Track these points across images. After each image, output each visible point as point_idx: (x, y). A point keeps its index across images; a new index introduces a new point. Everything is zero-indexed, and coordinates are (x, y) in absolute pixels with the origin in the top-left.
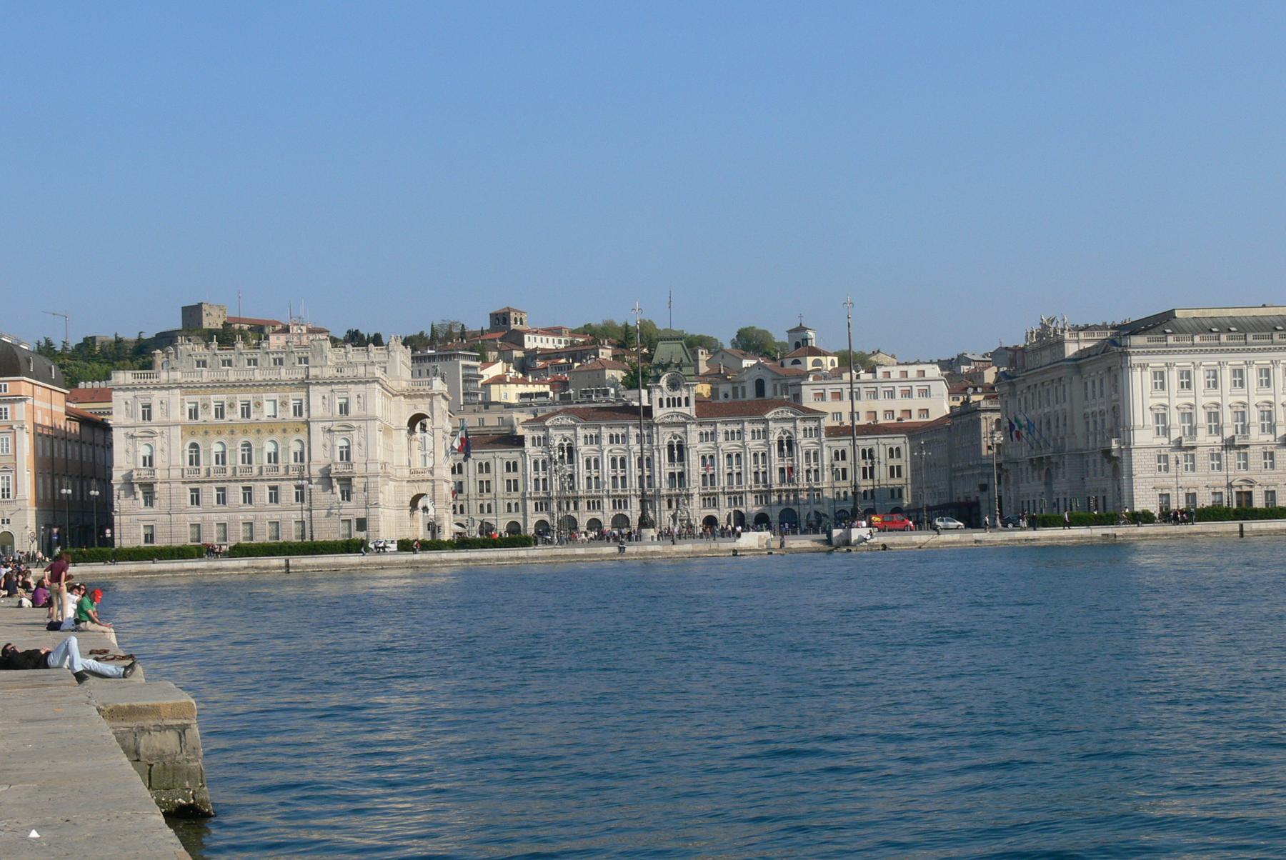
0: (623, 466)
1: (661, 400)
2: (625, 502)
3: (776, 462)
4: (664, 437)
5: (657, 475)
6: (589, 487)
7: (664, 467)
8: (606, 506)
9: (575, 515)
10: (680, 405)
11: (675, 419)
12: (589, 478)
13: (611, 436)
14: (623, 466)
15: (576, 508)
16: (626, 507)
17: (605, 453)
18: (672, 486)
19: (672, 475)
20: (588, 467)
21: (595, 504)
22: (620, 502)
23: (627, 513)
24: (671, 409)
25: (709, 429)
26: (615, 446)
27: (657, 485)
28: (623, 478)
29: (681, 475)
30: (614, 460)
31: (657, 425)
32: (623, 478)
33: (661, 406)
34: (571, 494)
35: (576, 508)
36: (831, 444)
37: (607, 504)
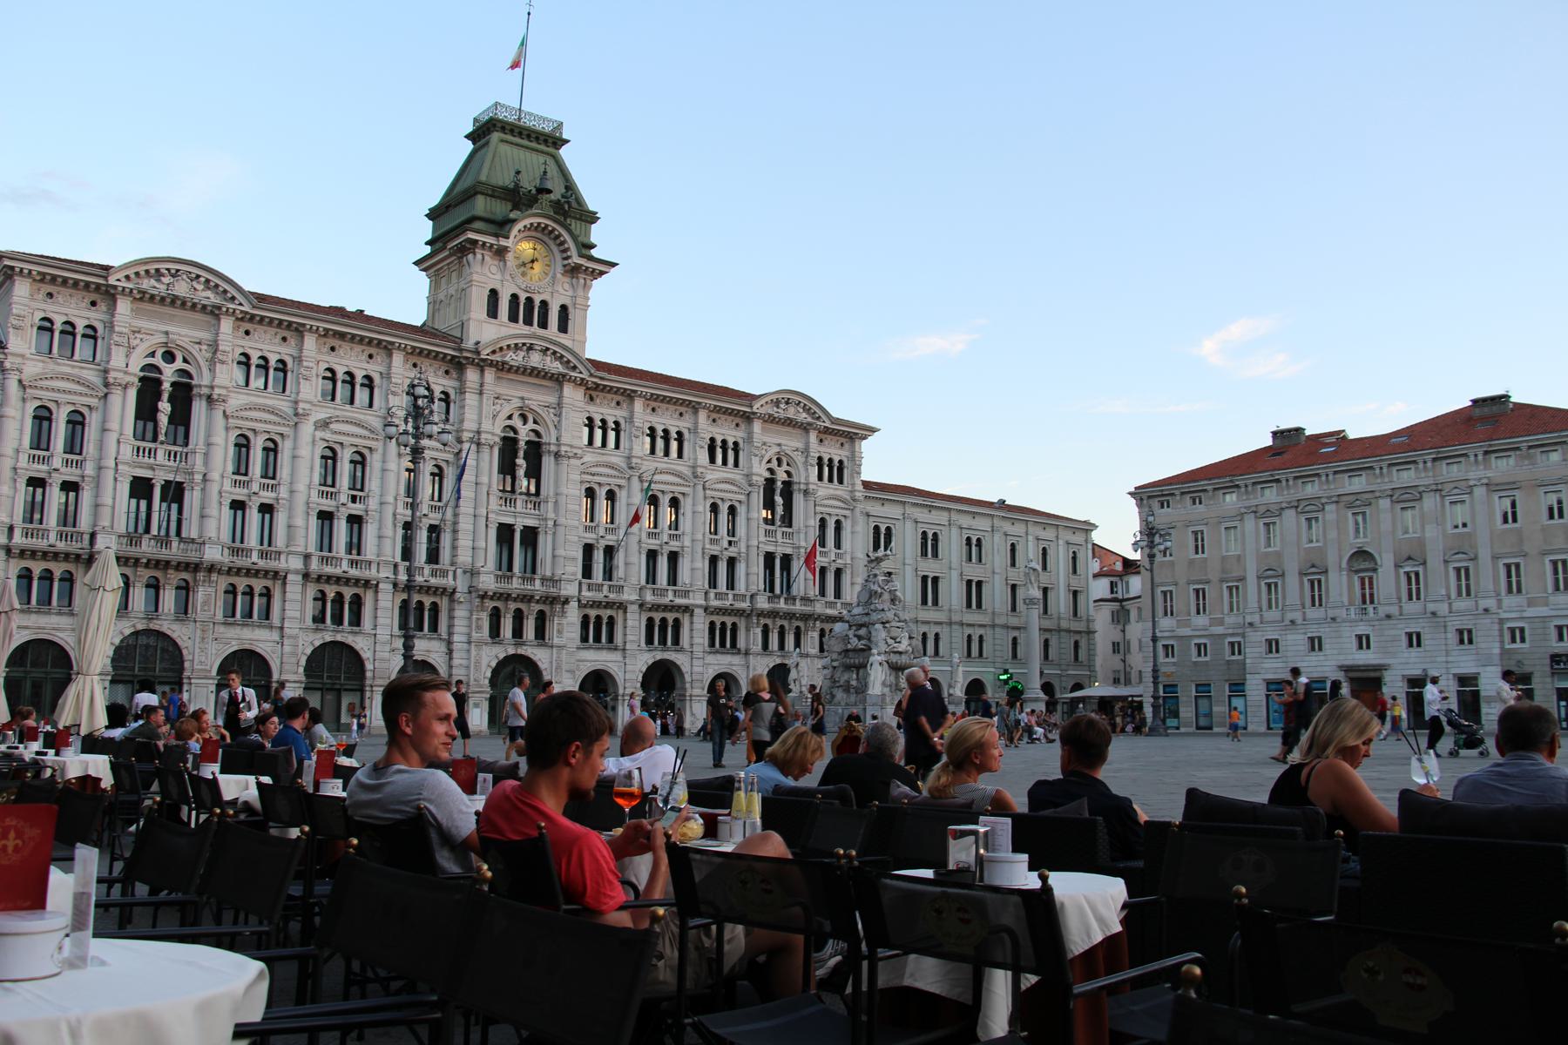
0: (358, 484)
1: (494, 294)
2: (357, 602)
3: (755, 534)
4: (487, 410)
5: (465, 524)
6: (239, 532)
7: (481, 504)
8: (292, 611)
9: (178, 632)
10: (544, 324)
11: (535, 360)
12: (238, 506)
13: (331, 375)
14: (358, 484)
15: (184, 609)
16: (356, 620)
17: (307, 429)
18: (505, 564)
19: (505, 533)
20: (242, 468)
21: (252, 593)
22: (341, 603)
23: (361, 644)
24: (520, 328)
25: (611, 413)
26: (340, 409)
27: (464, 557)
28: (355, 521)
29: (531, 536)
30: (330, 457)
31: (482, 365)
32: (355, 521)
33: (493, 312)
34: (175, 551)
35: (184, 609)
36: (876, 509)
37: (296, 604)
